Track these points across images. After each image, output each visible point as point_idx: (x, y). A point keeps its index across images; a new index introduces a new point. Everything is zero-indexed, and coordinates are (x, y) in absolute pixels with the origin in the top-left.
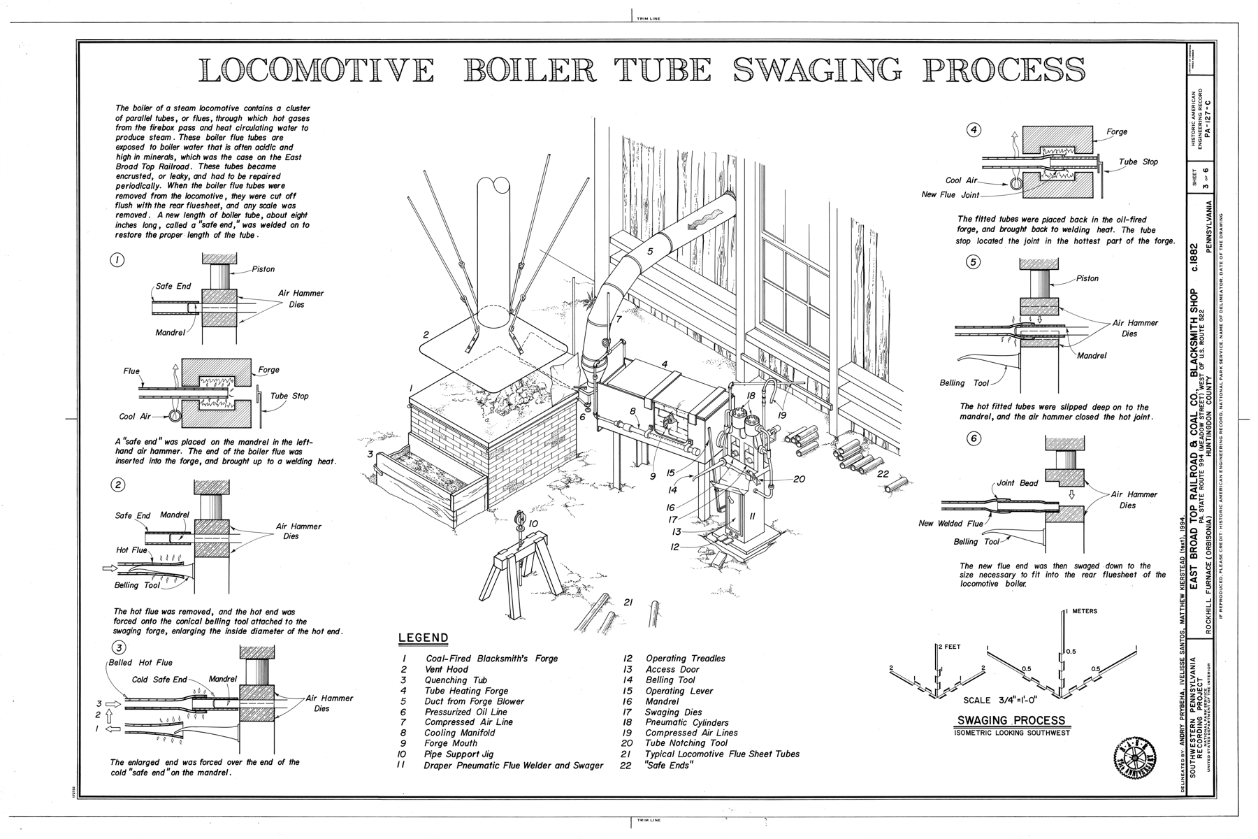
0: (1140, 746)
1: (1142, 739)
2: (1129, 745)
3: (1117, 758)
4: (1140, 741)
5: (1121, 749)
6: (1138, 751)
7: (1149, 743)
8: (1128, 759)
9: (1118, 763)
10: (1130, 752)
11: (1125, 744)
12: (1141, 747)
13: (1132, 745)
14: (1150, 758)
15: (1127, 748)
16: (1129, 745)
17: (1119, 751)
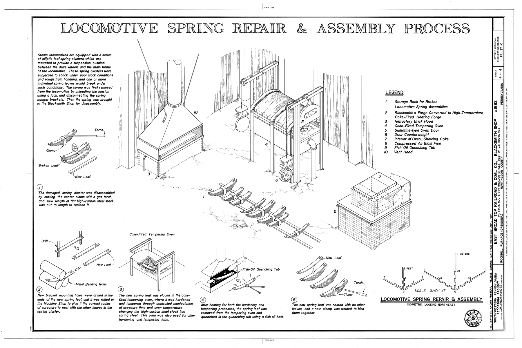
0: (475, 313)
2: (471, 313)
4: (475, 312)
6: (474, 315)
10: (471, 316)
11: (469, 312)
13: (472, 313)
15: (470, 314)
16: (471, 313)
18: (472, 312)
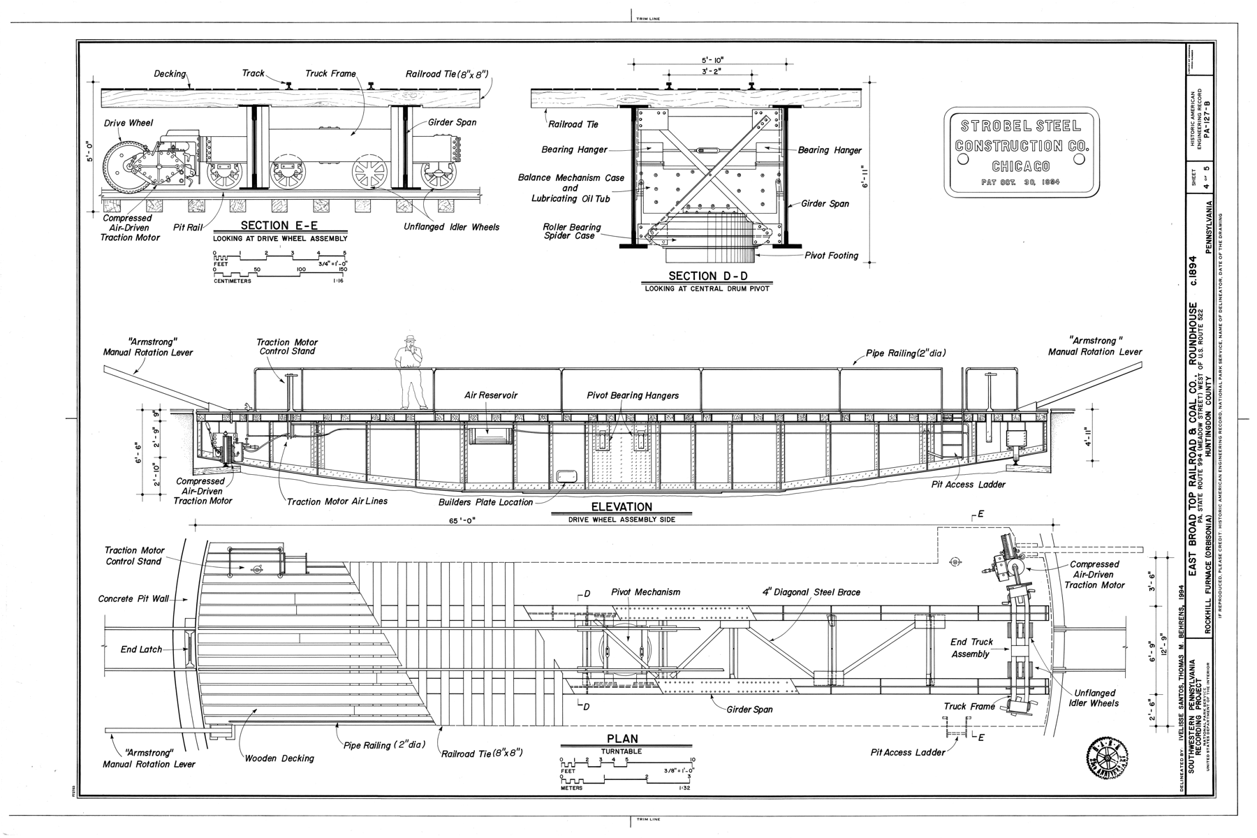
1: (1115, 739)
2: (1103, 745)
3: (1090, 758)
4: (1114, 742)
5: (1095, 749)
6: (1111, 751)
7: (1122, 744)
8: (1100, 759)
9: (1090, 762)
11: (1099, 743)
12: (1114, 747)
13: (1106, 745)
14: (1123, 759)
16: (1103, 745)
17: (1092, 750)
18: (1104, 744)
